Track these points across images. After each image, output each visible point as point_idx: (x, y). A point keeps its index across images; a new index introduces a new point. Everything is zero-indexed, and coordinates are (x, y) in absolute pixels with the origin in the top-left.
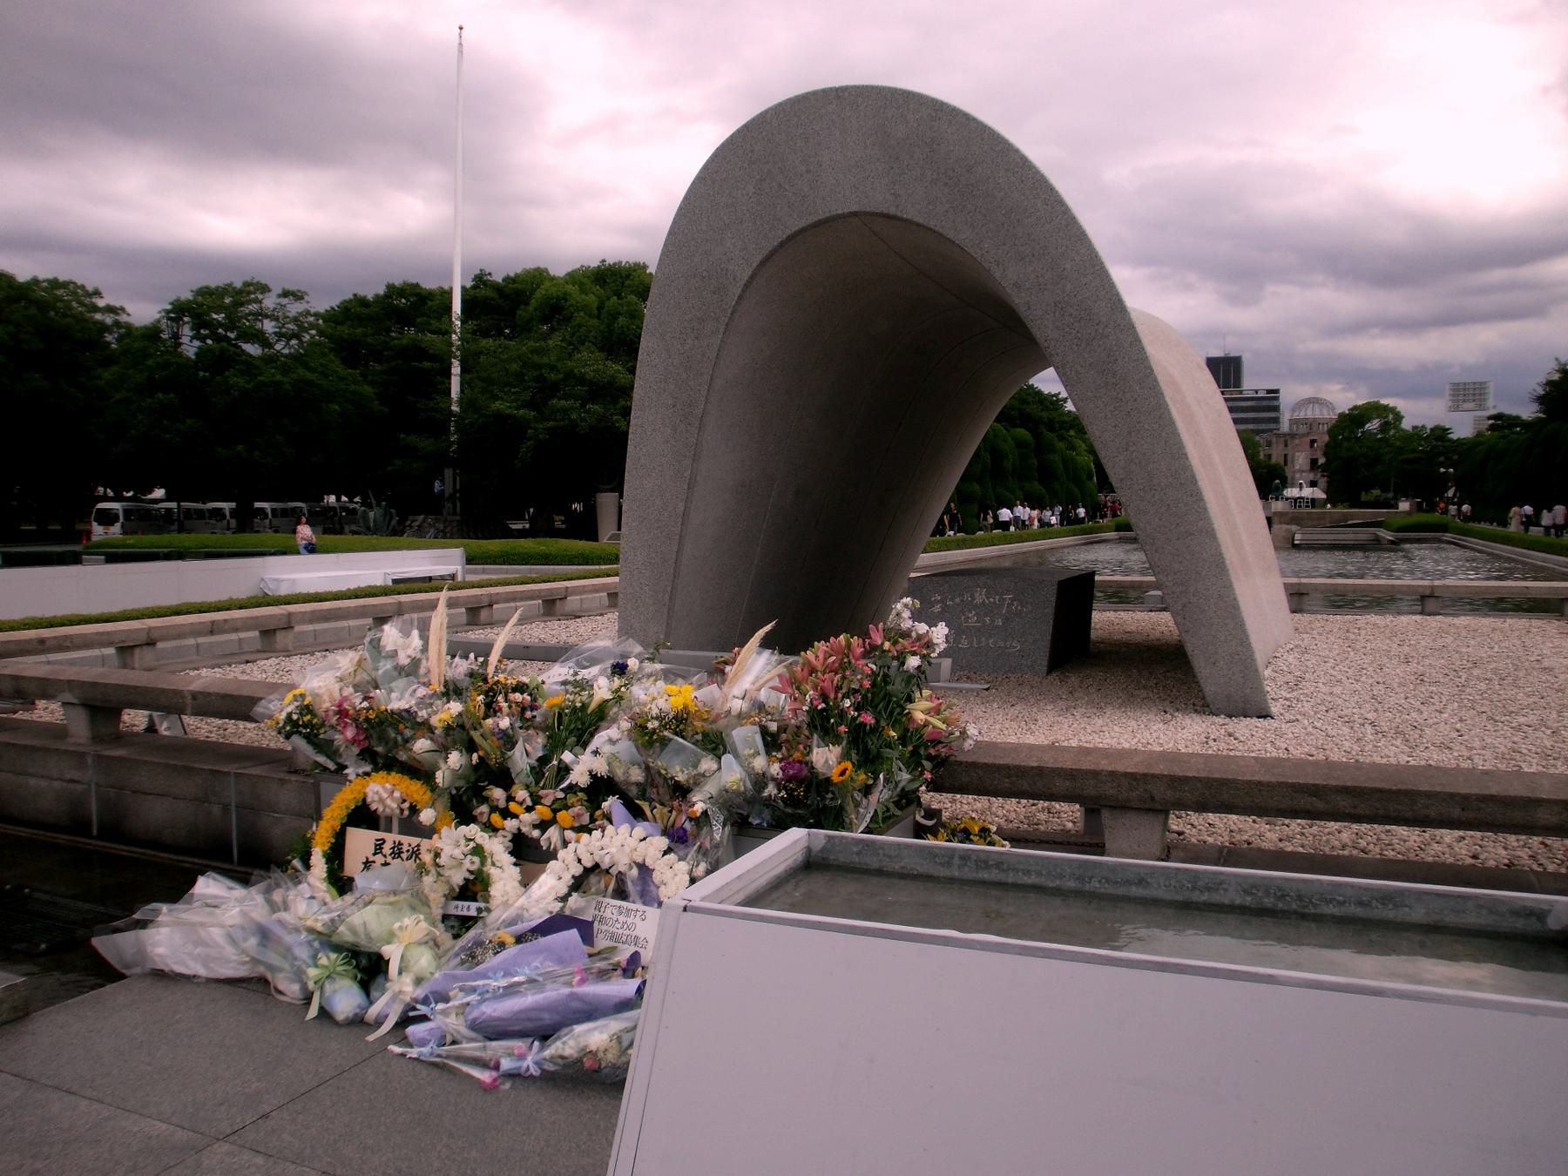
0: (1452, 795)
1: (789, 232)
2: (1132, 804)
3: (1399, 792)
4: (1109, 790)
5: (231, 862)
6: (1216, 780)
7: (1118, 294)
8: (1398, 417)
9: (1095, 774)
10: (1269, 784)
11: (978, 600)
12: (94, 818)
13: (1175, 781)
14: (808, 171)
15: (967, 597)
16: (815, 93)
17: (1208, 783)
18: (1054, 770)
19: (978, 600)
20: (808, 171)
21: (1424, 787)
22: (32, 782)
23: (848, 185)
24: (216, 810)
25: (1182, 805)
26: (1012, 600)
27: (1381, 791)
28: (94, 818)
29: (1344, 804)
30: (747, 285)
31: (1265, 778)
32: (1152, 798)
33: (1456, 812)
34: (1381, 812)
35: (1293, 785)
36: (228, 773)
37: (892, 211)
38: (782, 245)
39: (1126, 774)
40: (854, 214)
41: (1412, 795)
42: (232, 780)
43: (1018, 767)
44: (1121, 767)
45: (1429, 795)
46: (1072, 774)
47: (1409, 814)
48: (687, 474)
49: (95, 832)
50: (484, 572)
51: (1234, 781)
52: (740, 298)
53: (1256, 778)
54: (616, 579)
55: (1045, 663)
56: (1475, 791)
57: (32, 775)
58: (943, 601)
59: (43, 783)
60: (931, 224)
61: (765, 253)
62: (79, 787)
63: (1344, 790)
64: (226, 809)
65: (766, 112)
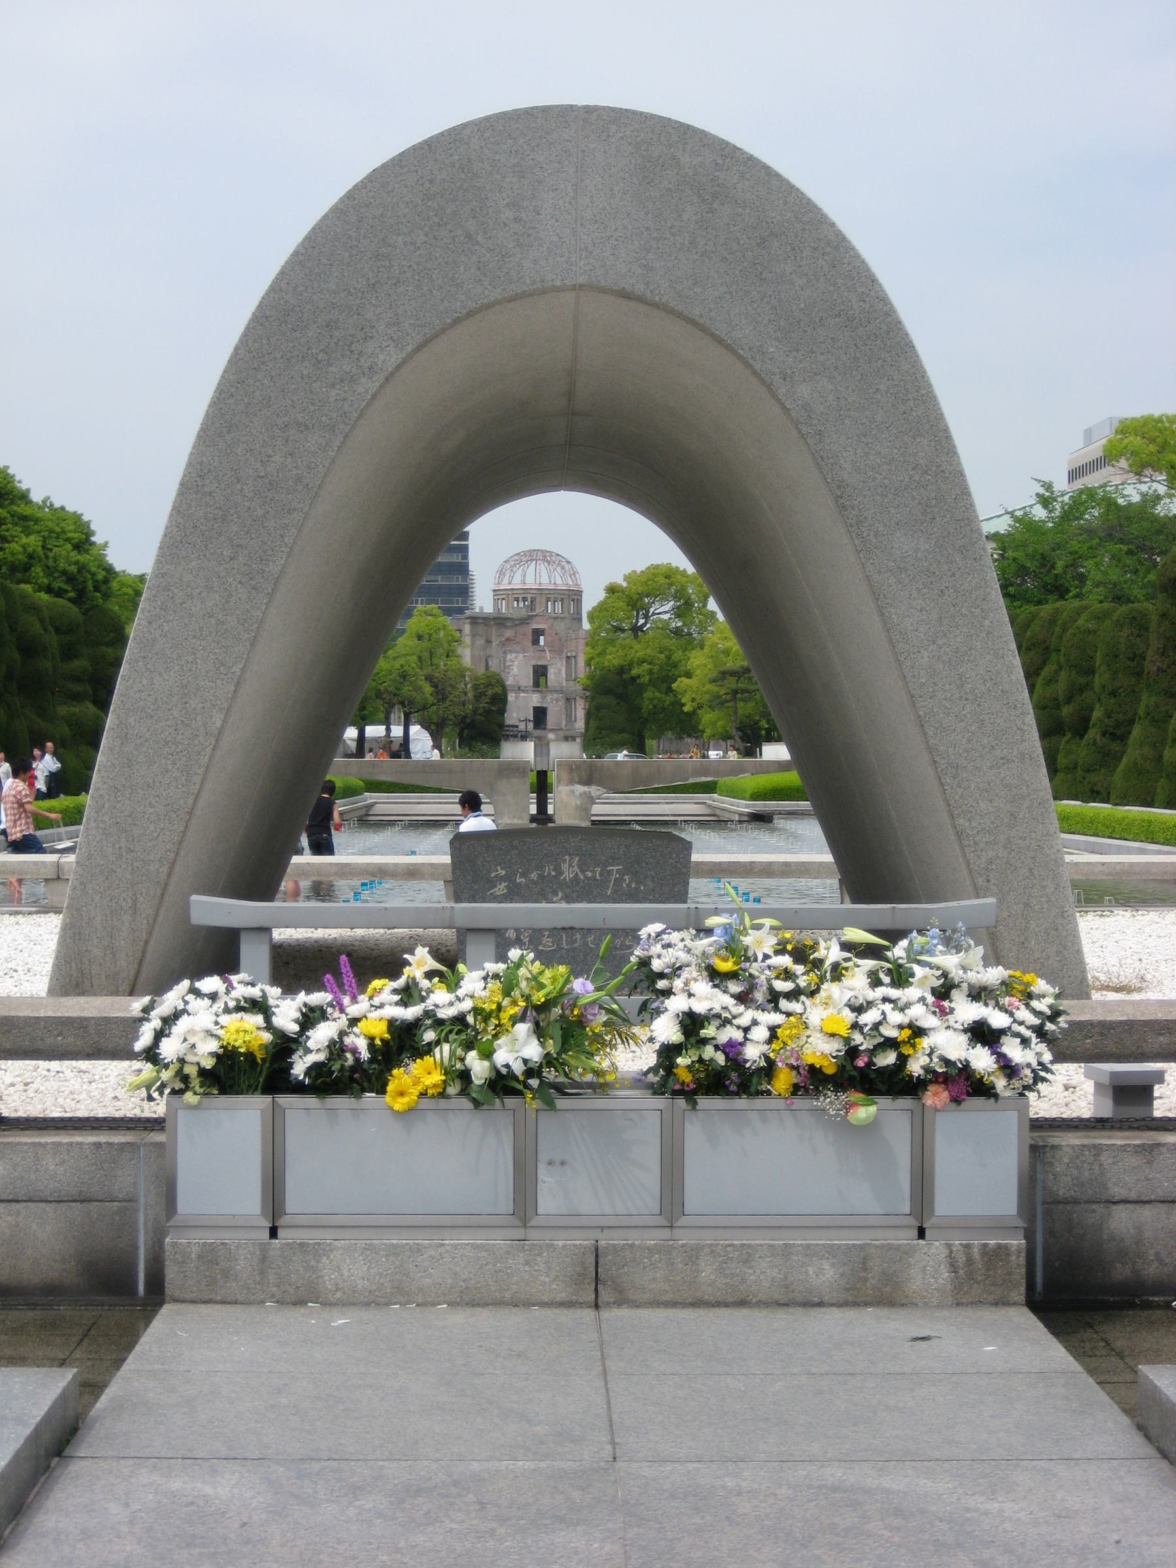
7: (946, 430)
14: (517, 220)
15: (549, 870)
16: (545, 110)
20: (517, 220)
26: (622, 873)
37: (640, 288)
38: (456, 322)
43: (1103, 1024)
48: (237, 669)
52: (374, 397)
58: (508, 878)
60: (696, 312)
65: (464, 126)
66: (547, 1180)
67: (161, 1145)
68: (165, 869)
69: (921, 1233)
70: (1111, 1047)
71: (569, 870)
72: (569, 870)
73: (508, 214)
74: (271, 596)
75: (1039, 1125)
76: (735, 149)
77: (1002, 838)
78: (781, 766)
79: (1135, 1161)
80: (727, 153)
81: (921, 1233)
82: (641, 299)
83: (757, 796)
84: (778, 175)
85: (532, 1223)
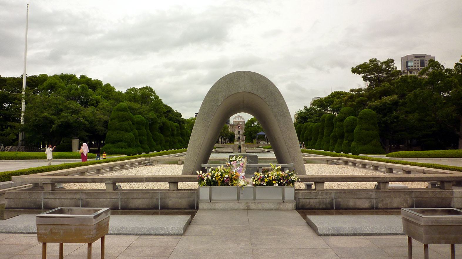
4: (318, 180)
5: (158, 209)
12: (120, 205)
14: (237, 84)
17: (331, 178)
22: (101, 200)
23: (245, 86)
24: (155, 200)
28: (120, 205)
32: (323, 181)
33: (361, 180)
36: (159, 192)
37: (251, 92)
42: (159, 193)
47: (356, 181)
49: (120, 208)
50: (68, 161)
54: (185, 158)
57: (100, 198)
59: (104, 200)
62: (116, 199)
66: (241, 195)
67: (198, 192)
68: (196, 160)
69: (283, 202)
73: (236, 83)
74: (208, 128)
75: (297, 190)
76: (262, 76)
77: (295, 156)
79: (309, 194)
81: (283, 202)
82: (251, 93)
83: (268, 149)
85: (240, 200)
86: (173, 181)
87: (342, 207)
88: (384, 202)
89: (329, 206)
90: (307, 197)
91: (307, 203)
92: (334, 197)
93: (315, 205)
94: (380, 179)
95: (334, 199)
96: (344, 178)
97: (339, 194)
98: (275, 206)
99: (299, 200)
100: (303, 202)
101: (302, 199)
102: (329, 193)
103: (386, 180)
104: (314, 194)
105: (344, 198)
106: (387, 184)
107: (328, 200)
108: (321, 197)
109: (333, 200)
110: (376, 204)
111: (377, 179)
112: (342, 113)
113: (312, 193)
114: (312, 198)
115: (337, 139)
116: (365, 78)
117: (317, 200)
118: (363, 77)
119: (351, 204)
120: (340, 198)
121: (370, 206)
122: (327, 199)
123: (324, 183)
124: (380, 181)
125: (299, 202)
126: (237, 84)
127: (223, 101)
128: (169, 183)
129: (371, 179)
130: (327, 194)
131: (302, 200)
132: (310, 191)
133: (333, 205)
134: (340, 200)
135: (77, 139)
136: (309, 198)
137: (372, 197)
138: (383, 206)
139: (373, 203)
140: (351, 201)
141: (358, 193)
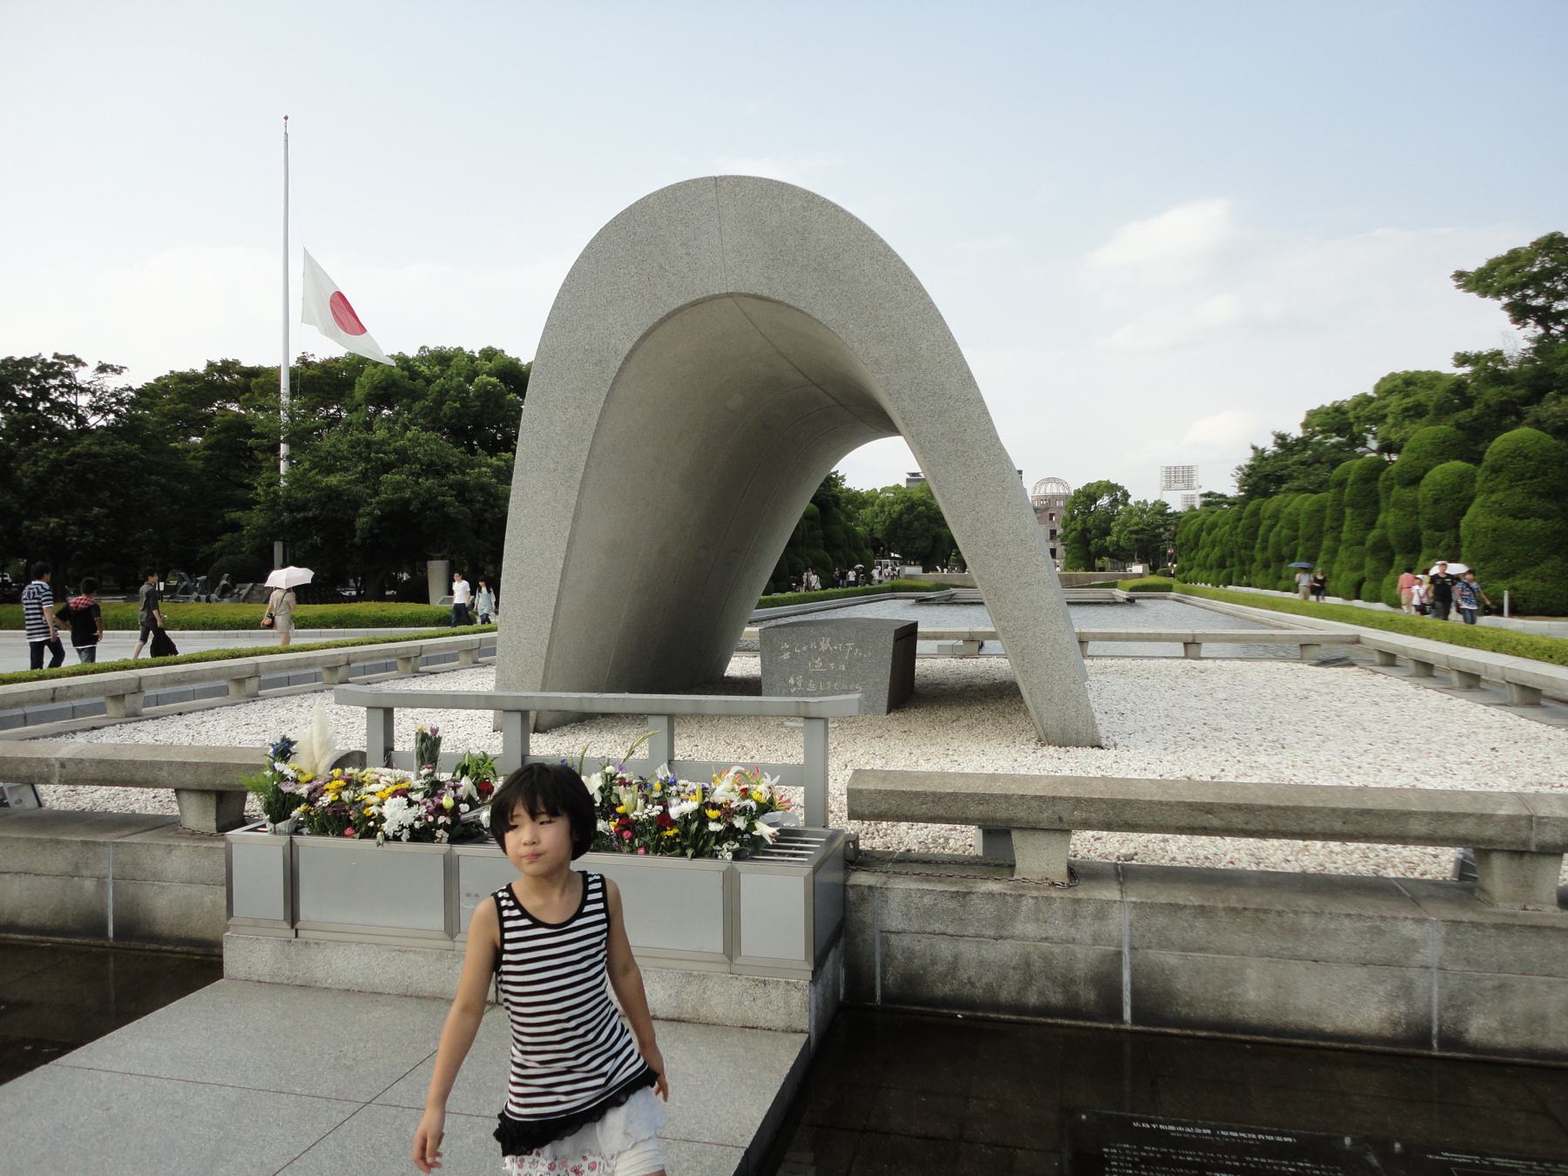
0: (1334, 810)
1: (668, 310)
2: (1042, 825)
3: (1286, 809)
4: (1021, 813)
6: (1120, 801)
8: (1126, 495)
9: (1007, 797)
10: (1167, 804)
11: (823, 647)
13: (1078, 802)
14: (688, 254)
15: (813, 645)
16: (695, 181)
17: (1113, 804)
18: (967, 795)
19: (823, 647)
21: (1309, 803)
24: (89, 885)
25: (1086, 825)
27: (1270, 807)
29: (1238, 820)
30: (628, 359)
31: (1165, 798)
32: (1060, 819)
33: (1338, 826)
34: (1271, 827)
35: (1190, 805)
37: (766, 293)
38: (662, 321)
39: (1035, 797)
40: (729, 295)
41: (1297, 811)
43: (934, 794)
44: (1030, 791)
45: (1314, 810)
46: (983, 799)
47: (1296, 829)
50: (320, 635)
51: (1137, 801)
52: (621, 369)
53: (1156, 798)
55: (885, 703)
56: (1353, 805)
61: (645, 328)
63: (1238, 807)
64: (101, 881)
65: (649, 196)
70: (941, 812)
71: (824, 645)
72: (824, 645)
73: (682, 251)
78: (1141, 576)
79: (952, 905)
80: (811, 200)
84: (843, 211)
86: (188, 779)
87: (1184, 1011)
88: (1518, 1005)
89: (1088, 995)
90: (937, 927)
91: (940, 968)
92: (1126, 940)
93: (990, 985)
94: (1490, 831)
95: (1126, 950)
96: (1209, 809)
97: (1161, 920)
98: (673, 992)
99: (885, 942)
100: (910, 955)
101: (903, 932)
102: (1091, 908)
103: (1536, 838)
104: (988, 909)
105: (1201, 949)
106: (1547, 864)
107: (1085, 957)
108: (1031, 929)
109: (1119, 953)
110: (1452, 1014)
111: (1463, 829)
112: (1413, 451)
113: (975, 900)
114: (971, 931)
115: (1393, 555)
116: (1520, 313)
117: (1006, 951)
118: (1507, 307)
119: (1252, 995)
120: (1168, 944)
121: (1395, 1024)
122: (1077, 949)
123: (1068, 832)
124: (1490, 841)
125: (888, 957)
126: (688, 254)
127: (629, 346)
128: (177, 791)
129: (1416, 827)
130: (1075, 914)
131: (906, 941)
132: (962, 889)
133: (1121, 991)
134: (1171, 959)
135: (442, 558)
136: (950, 931)
137: (1418, 958)
138: (1506, 1030)
139: (1420, 1005)
140: (1252, 974)
141: (1307, 920)
